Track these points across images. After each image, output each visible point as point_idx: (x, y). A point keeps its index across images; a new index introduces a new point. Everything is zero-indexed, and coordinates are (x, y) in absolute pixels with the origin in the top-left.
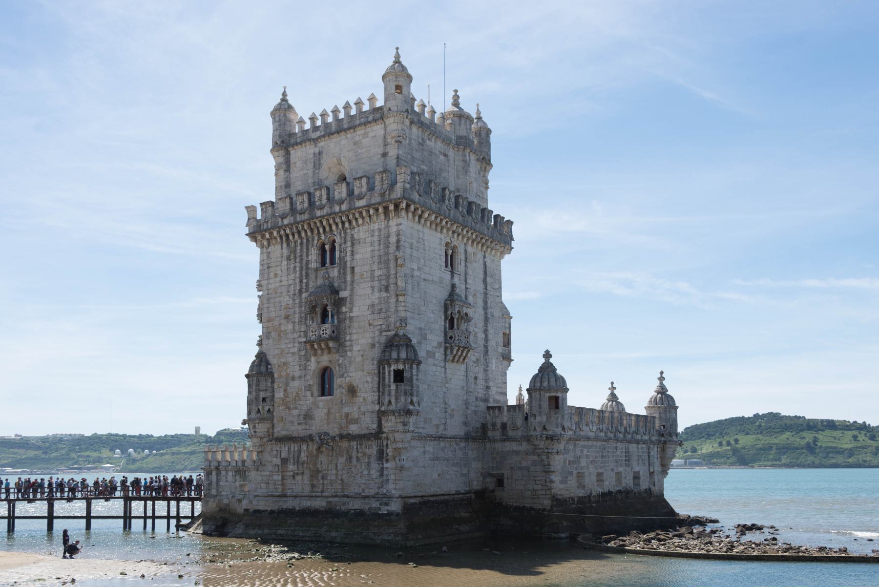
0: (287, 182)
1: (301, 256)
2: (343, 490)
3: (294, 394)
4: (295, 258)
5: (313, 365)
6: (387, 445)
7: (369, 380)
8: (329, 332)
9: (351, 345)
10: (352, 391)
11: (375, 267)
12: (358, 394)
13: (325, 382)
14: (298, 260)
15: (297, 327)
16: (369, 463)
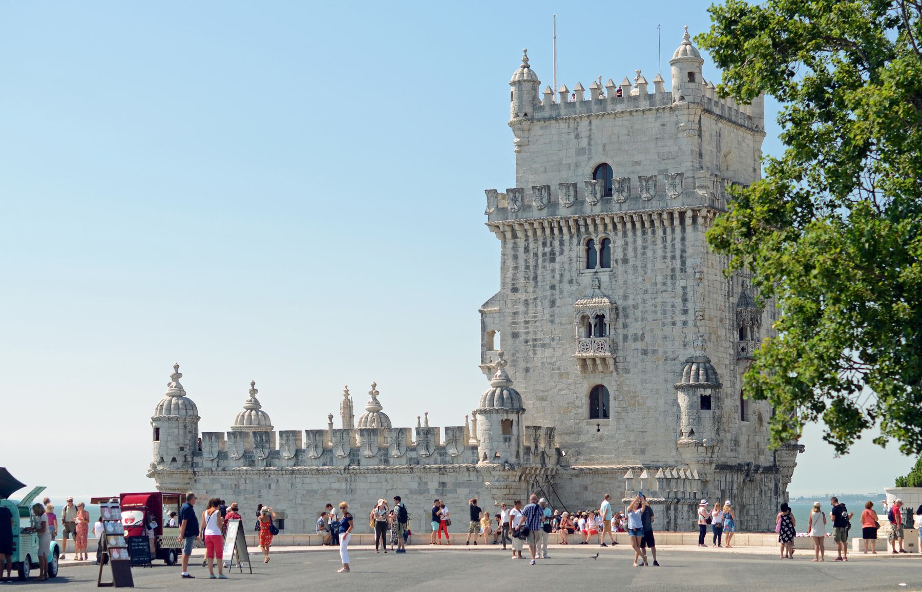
10: (760, 419)
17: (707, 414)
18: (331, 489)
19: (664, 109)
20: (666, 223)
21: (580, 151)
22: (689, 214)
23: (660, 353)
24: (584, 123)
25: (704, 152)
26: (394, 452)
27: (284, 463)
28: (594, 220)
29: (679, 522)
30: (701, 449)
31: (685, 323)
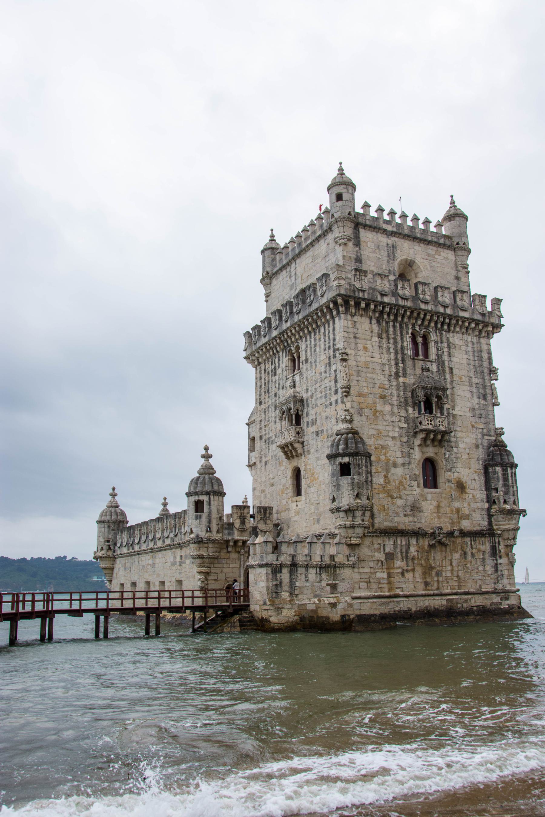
0: (357, 256)
1: (395, 339)
2: (460, 587)
3: (398, 482)
4: (388, 339)
5: (417, 455)
6: (499, 542)
7: (476, 478)
8: (445, 424)
9: (457, 442)
10: (461, 487)
11: (472, 374)
12: (467, 491)
13: (430, 473)
14: (391, 341)
15: (396, 410)
16: (484, 559)
17: (345, 481)
18: (148, 564)
19: (326, 231)
20: (323, 320)
21: (292, 286)
22: (331, 306)
23: (325, 432)
24: (293, 265)
25: (364, 258)
26: (165, 534)
27: (137, 548)
28: (287, 333)
29: (298, 584)
30: (342, 514)
31: (336, 402)
